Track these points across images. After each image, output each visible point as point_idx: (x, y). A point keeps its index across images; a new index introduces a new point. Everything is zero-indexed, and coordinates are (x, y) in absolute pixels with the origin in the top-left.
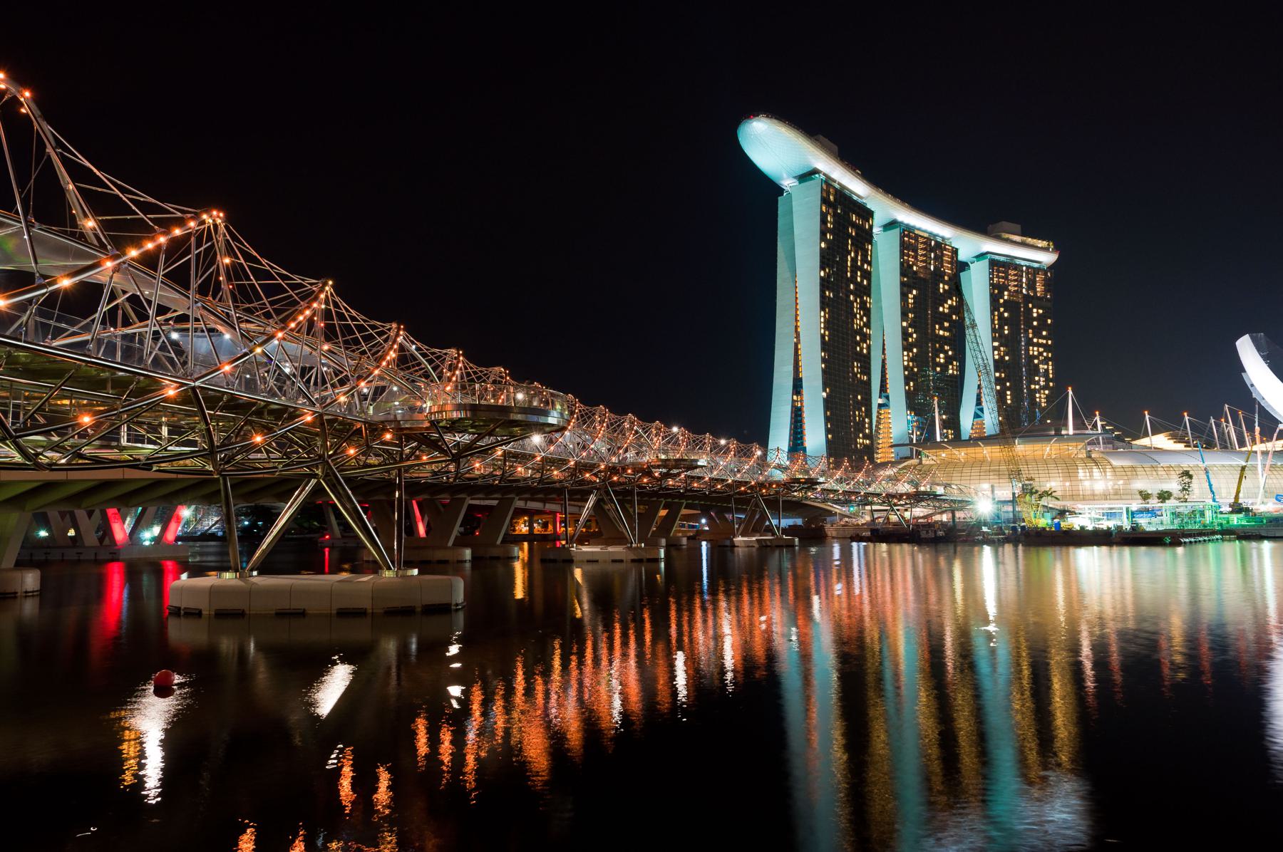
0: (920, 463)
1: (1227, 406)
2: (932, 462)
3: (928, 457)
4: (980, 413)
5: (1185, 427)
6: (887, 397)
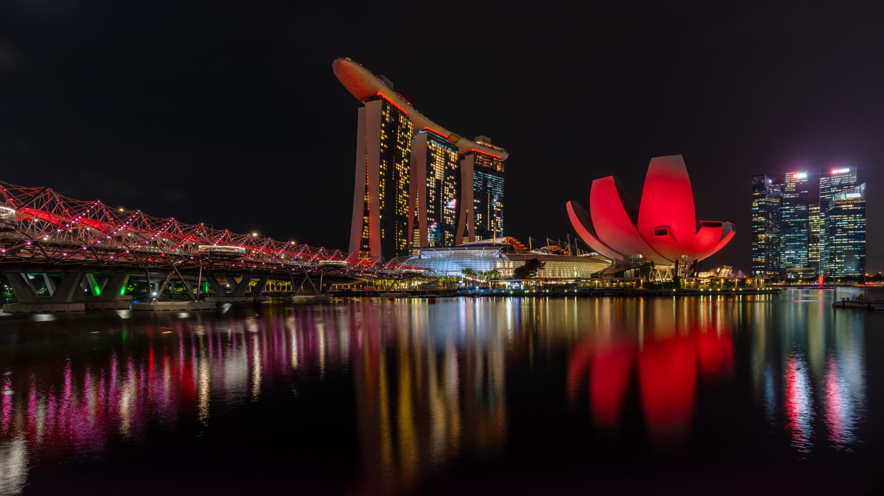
0: (420, 258)
1: (568, 235)
2: (427, 258)
4: (466, 233)
6: (418, 223)
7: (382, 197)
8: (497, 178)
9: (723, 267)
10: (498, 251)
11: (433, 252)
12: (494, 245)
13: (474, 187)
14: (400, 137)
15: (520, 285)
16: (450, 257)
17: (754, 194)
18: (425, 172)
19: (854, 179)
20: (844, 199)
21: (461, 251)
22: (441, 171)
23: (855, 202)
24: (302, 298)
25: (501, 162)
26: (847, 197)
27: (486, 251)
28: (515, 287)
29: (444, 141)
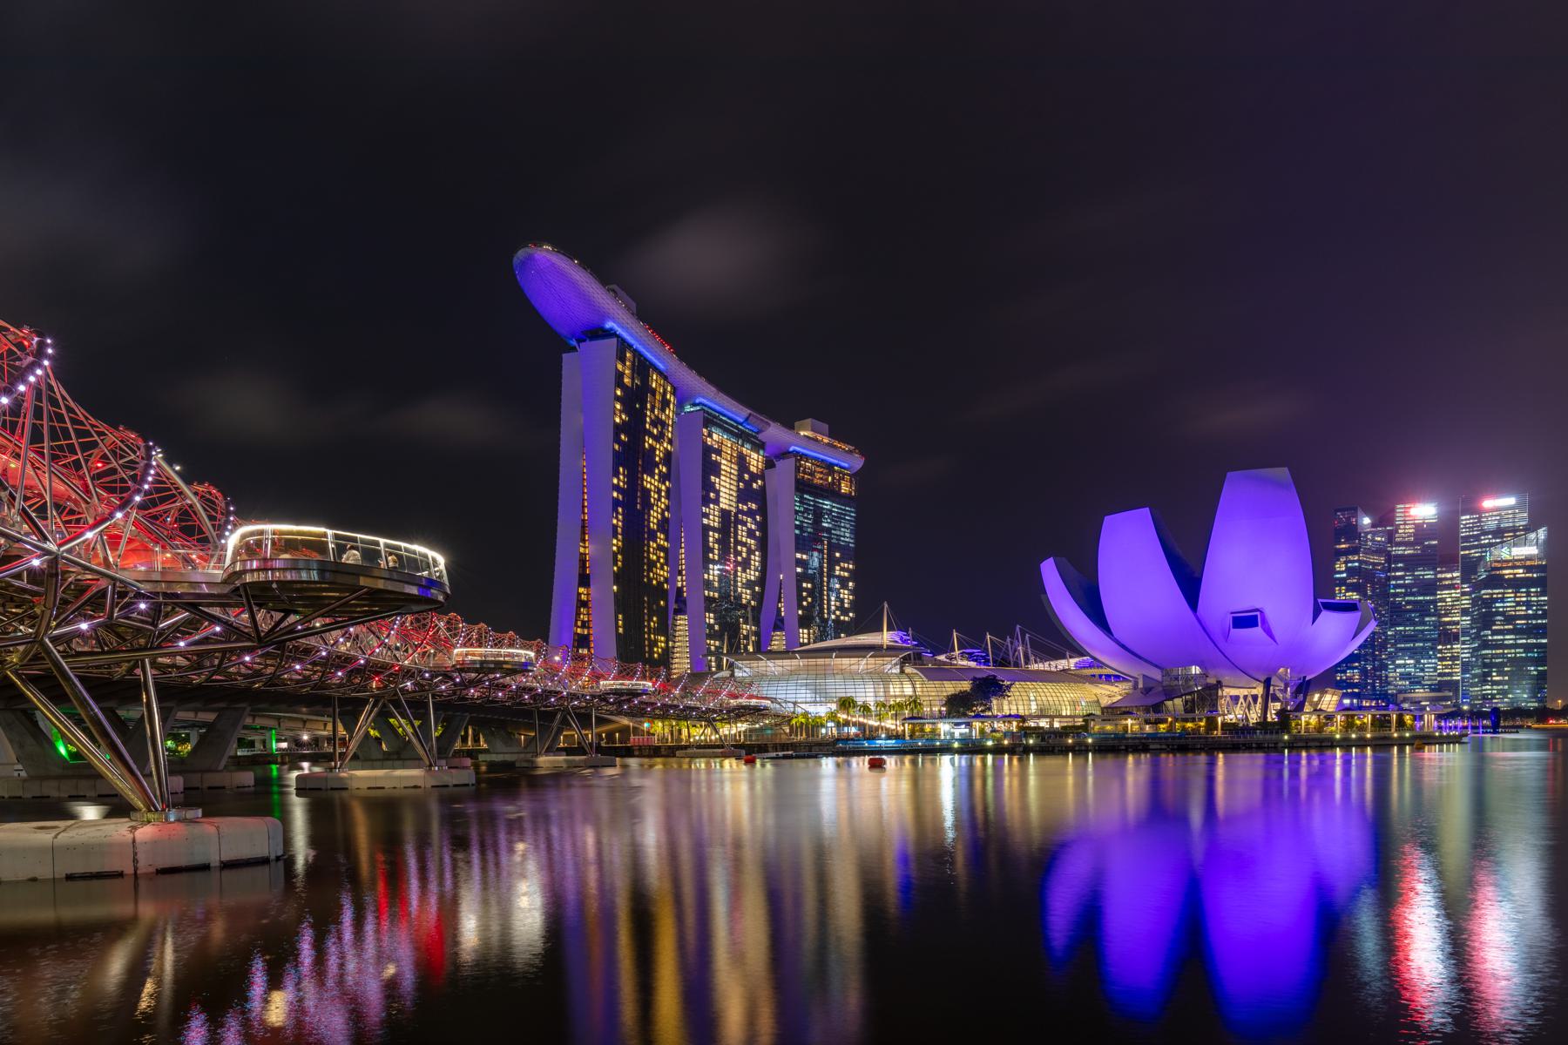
0: (732, 675)
1: (1018, 626)
2: (745, 675)
3: (740, 668)
4: (778, 623)
5: (987, 644)
7: (617, 546)
8: (841, 509)
9: (1326, 692)
10: (895, 660)
11: (761, 663)
12: (885, 647)
13: (797, 527)
14: (651, 418)
15: (971, 731)
16: (791, 673)
17: (1338, 546)
18: (699, 493)
19: (1522, 519)
20: (1508, 558)
21: (820, 661)
22: (731, 492)
23: (1528, 563)
24: (558, 762)
25: (847, 474)
26: (1513, 554)
27: (872, 661)
28: (961, 734)
29: (737, 428)
